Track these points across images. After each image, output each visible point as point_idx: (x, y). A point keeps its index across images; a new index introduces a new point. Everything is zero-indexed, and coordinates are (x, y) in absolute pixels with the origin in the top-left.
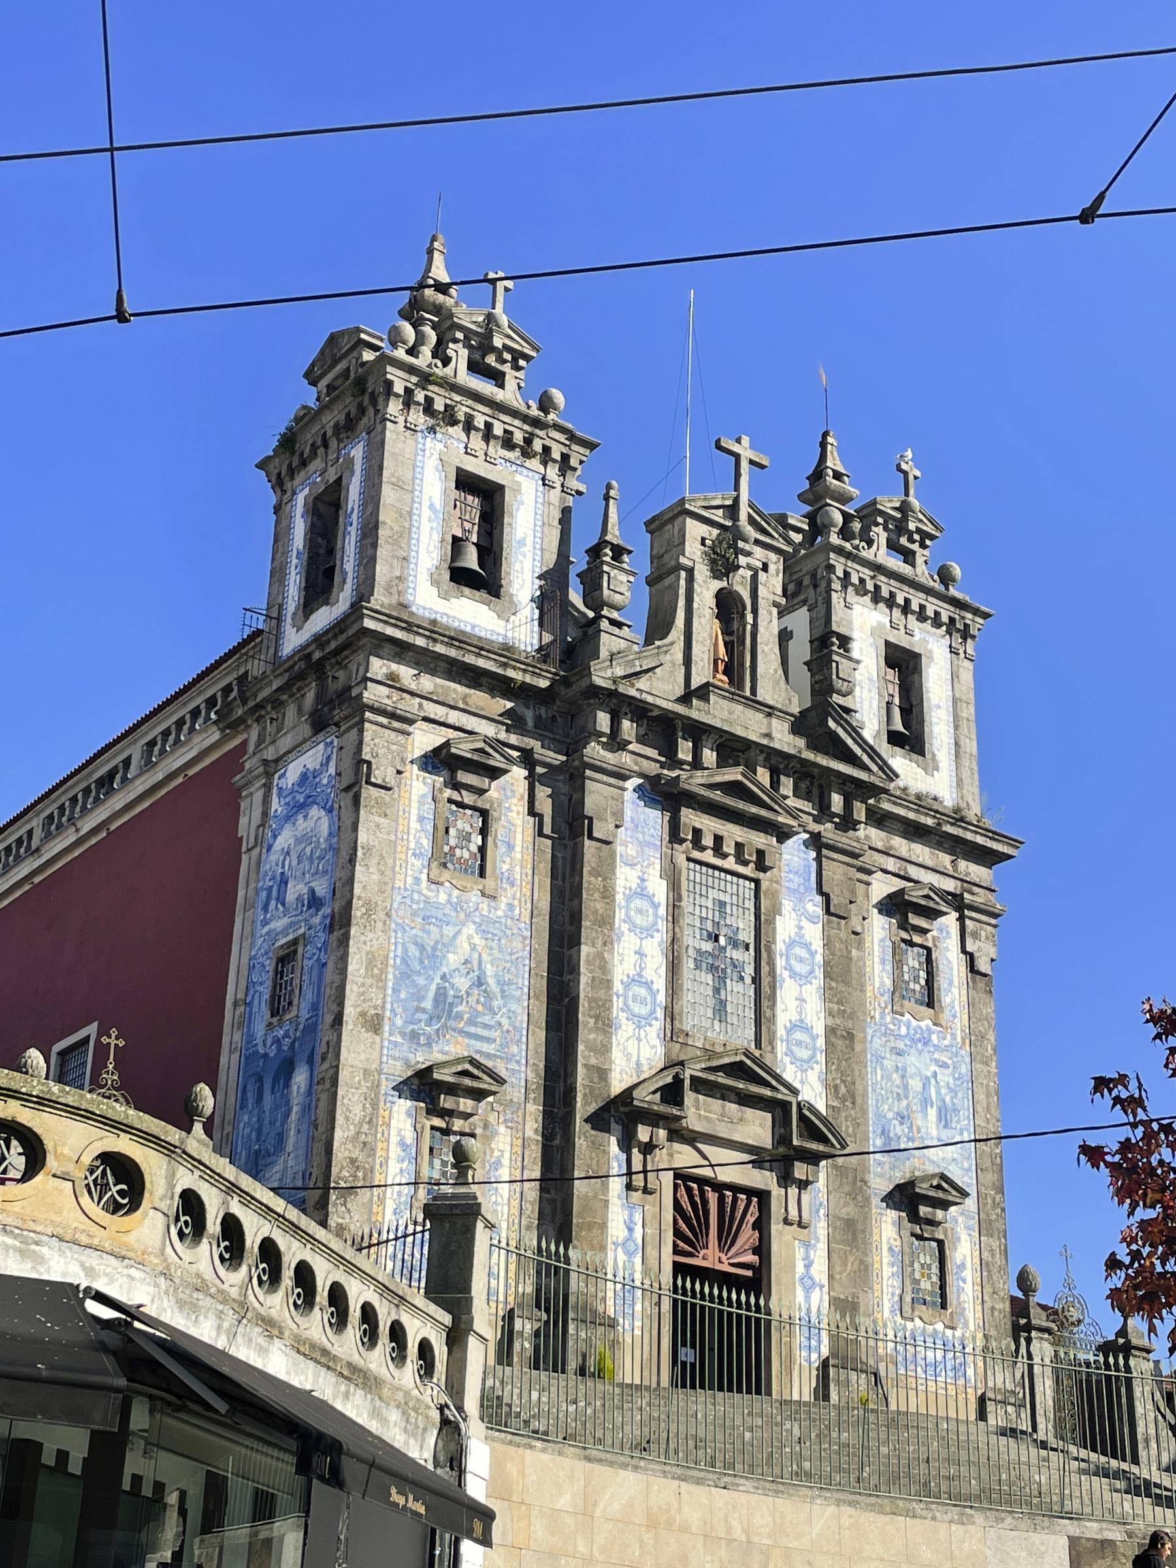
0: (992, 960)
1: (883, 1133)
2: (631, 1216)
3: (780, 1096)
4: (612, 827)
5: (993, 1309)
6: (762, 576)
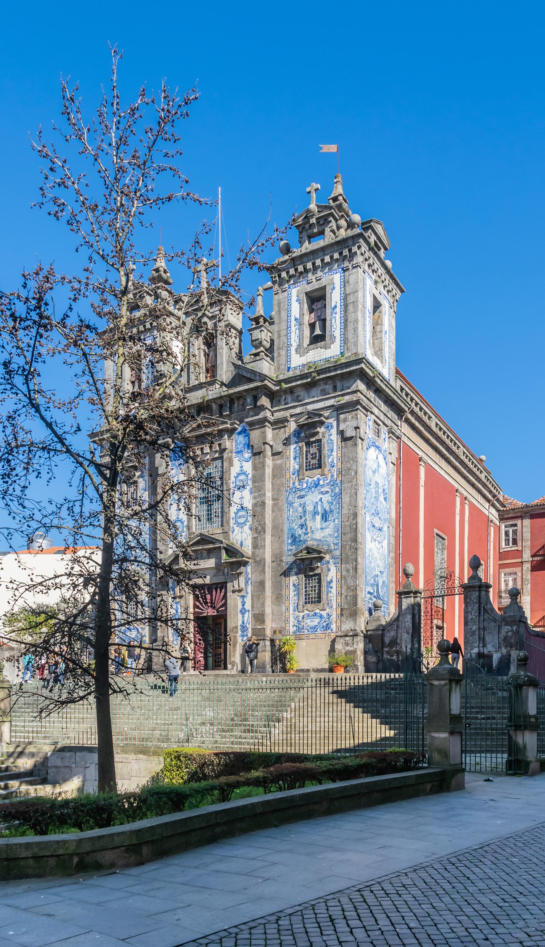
1: (292, 536)
5: (346, 597)
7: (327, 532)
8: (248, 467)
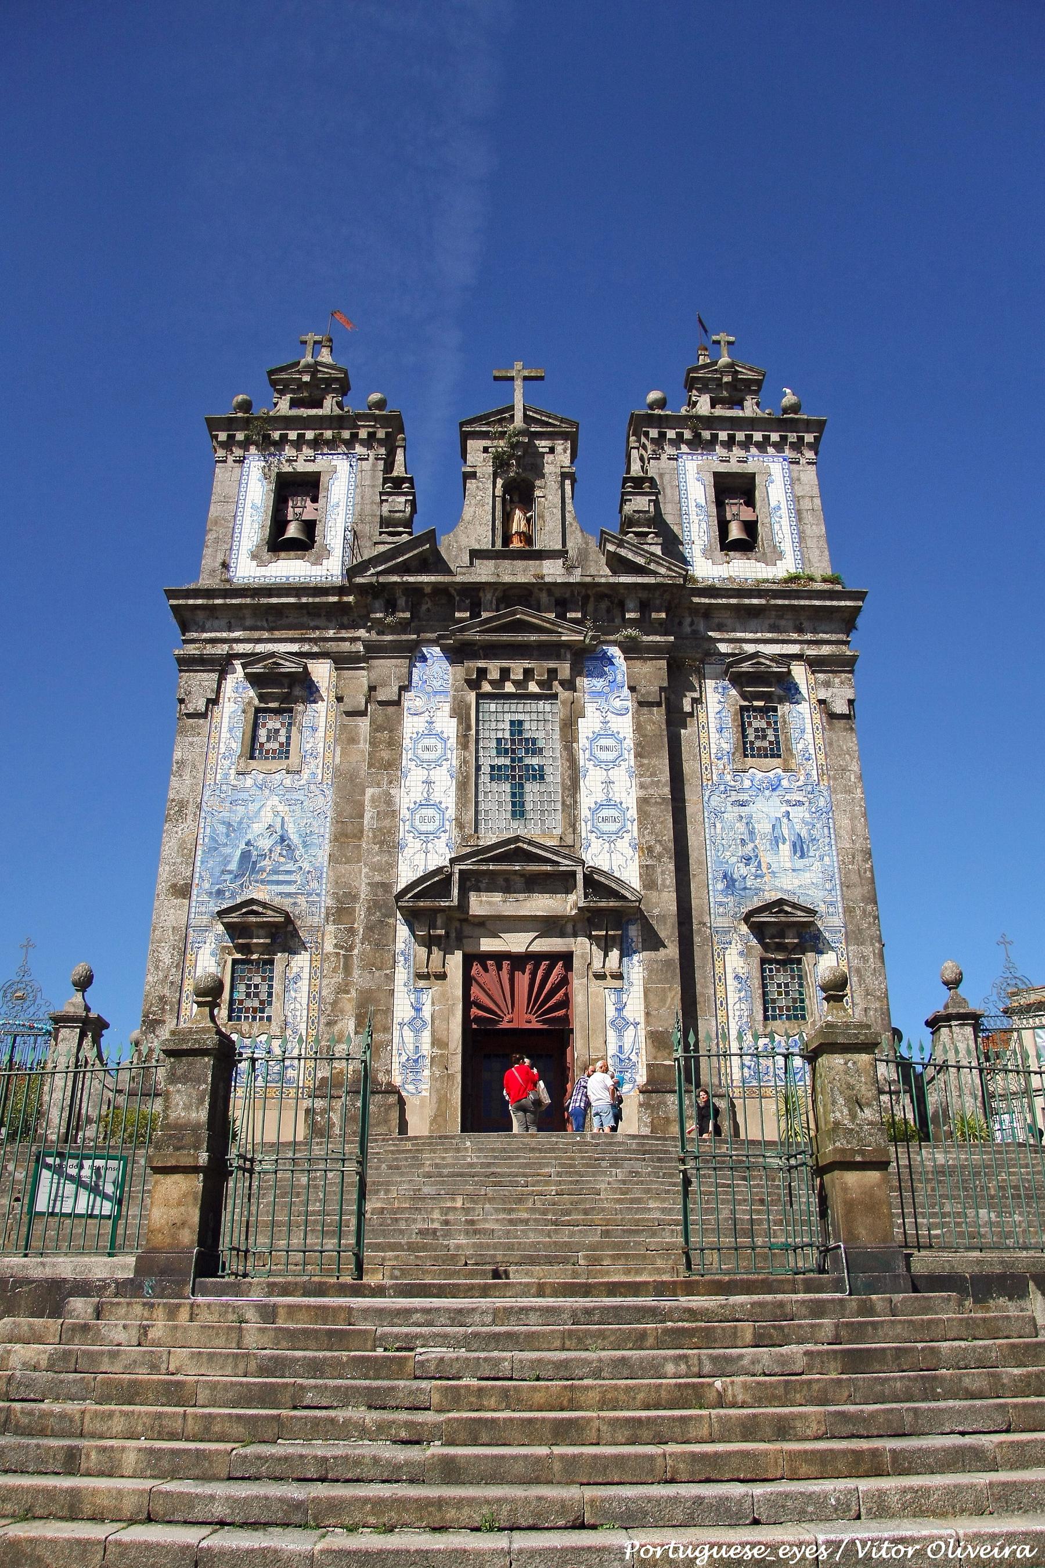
0: (851, 702)
1: (725, 877)
2: (417, 1000)
3: (561, 868)
4: (396, 689)
5: (866, 1010)
7: (807, 877)
8: (624, 726)
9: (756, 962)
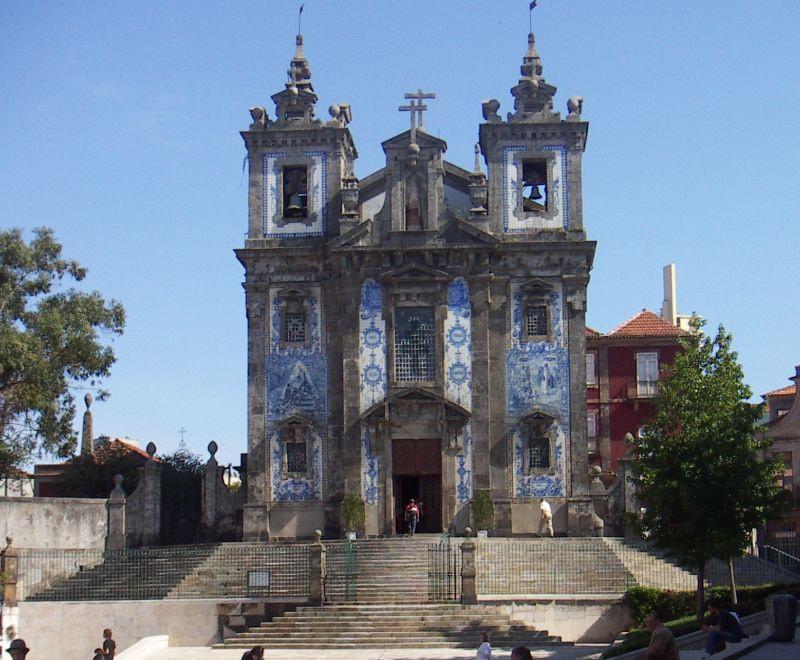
5: (577, 463)
6: (430, 164)
7: (554, 398)
8: (466, 323)
9: (526, 439)
